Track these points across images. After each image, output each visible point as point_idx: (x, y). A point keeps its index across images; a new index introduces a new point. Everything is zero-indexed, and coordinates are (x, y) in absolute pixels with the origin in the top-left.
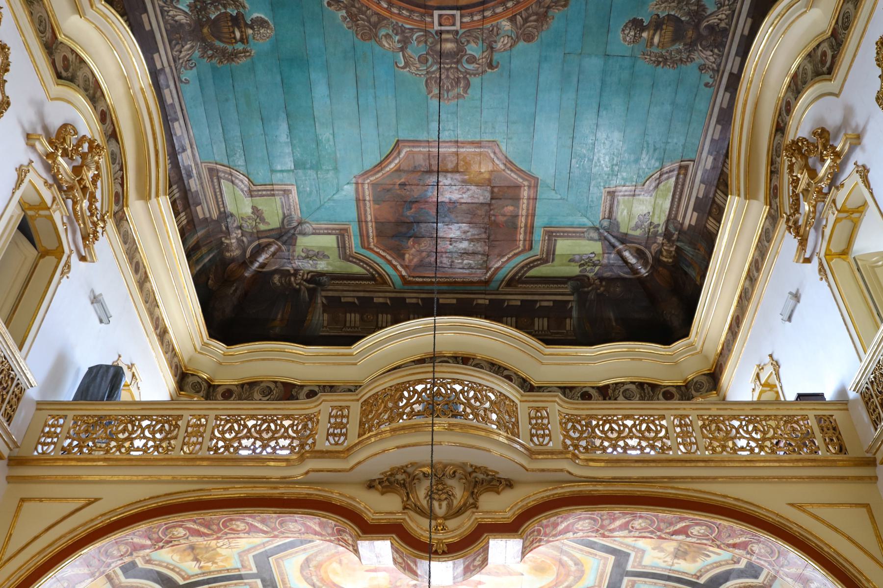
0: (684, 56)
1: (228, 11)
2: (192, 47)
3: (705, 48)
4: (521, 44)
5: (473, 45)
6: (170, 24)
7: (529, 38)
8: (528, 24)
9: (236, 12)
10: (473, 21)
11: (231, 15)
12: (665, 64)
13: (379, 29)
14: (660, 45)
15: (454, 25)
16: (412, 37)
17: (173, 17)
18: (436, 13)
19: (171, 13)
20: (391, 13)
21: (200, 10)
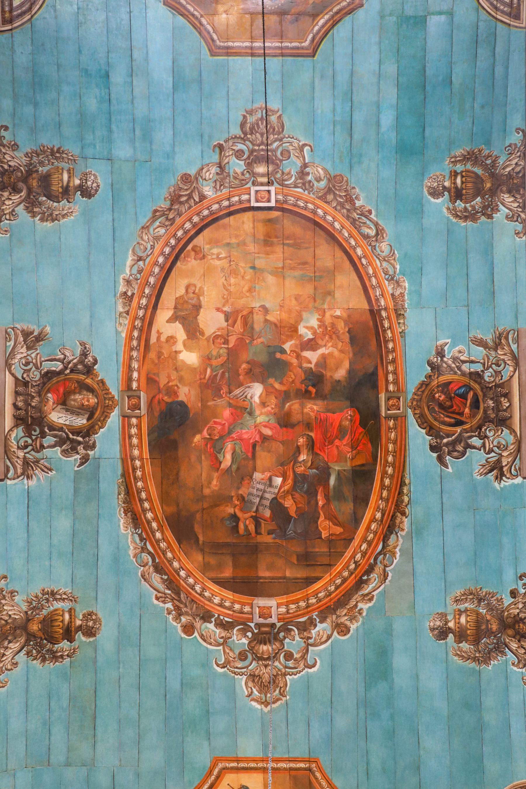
0: (35, 159)
1: (463, 205)
2: (504, 169)
3: (16, 169)
4: (193, 172)
5: (239, 170)
6: (520, 194)
7: (186, 178)
8: (188, 192)
9: (456, 204)
10: (239, 195)
11: (461, 201)
12: (52, 150)
13: (325, 188)
14: (61, 171)
15: (257, 192)
16: (296, 179)
17: (515, 201)
18: (273, 204)
19: (516, 205)
20: (313, 203)
21: (489, 206)
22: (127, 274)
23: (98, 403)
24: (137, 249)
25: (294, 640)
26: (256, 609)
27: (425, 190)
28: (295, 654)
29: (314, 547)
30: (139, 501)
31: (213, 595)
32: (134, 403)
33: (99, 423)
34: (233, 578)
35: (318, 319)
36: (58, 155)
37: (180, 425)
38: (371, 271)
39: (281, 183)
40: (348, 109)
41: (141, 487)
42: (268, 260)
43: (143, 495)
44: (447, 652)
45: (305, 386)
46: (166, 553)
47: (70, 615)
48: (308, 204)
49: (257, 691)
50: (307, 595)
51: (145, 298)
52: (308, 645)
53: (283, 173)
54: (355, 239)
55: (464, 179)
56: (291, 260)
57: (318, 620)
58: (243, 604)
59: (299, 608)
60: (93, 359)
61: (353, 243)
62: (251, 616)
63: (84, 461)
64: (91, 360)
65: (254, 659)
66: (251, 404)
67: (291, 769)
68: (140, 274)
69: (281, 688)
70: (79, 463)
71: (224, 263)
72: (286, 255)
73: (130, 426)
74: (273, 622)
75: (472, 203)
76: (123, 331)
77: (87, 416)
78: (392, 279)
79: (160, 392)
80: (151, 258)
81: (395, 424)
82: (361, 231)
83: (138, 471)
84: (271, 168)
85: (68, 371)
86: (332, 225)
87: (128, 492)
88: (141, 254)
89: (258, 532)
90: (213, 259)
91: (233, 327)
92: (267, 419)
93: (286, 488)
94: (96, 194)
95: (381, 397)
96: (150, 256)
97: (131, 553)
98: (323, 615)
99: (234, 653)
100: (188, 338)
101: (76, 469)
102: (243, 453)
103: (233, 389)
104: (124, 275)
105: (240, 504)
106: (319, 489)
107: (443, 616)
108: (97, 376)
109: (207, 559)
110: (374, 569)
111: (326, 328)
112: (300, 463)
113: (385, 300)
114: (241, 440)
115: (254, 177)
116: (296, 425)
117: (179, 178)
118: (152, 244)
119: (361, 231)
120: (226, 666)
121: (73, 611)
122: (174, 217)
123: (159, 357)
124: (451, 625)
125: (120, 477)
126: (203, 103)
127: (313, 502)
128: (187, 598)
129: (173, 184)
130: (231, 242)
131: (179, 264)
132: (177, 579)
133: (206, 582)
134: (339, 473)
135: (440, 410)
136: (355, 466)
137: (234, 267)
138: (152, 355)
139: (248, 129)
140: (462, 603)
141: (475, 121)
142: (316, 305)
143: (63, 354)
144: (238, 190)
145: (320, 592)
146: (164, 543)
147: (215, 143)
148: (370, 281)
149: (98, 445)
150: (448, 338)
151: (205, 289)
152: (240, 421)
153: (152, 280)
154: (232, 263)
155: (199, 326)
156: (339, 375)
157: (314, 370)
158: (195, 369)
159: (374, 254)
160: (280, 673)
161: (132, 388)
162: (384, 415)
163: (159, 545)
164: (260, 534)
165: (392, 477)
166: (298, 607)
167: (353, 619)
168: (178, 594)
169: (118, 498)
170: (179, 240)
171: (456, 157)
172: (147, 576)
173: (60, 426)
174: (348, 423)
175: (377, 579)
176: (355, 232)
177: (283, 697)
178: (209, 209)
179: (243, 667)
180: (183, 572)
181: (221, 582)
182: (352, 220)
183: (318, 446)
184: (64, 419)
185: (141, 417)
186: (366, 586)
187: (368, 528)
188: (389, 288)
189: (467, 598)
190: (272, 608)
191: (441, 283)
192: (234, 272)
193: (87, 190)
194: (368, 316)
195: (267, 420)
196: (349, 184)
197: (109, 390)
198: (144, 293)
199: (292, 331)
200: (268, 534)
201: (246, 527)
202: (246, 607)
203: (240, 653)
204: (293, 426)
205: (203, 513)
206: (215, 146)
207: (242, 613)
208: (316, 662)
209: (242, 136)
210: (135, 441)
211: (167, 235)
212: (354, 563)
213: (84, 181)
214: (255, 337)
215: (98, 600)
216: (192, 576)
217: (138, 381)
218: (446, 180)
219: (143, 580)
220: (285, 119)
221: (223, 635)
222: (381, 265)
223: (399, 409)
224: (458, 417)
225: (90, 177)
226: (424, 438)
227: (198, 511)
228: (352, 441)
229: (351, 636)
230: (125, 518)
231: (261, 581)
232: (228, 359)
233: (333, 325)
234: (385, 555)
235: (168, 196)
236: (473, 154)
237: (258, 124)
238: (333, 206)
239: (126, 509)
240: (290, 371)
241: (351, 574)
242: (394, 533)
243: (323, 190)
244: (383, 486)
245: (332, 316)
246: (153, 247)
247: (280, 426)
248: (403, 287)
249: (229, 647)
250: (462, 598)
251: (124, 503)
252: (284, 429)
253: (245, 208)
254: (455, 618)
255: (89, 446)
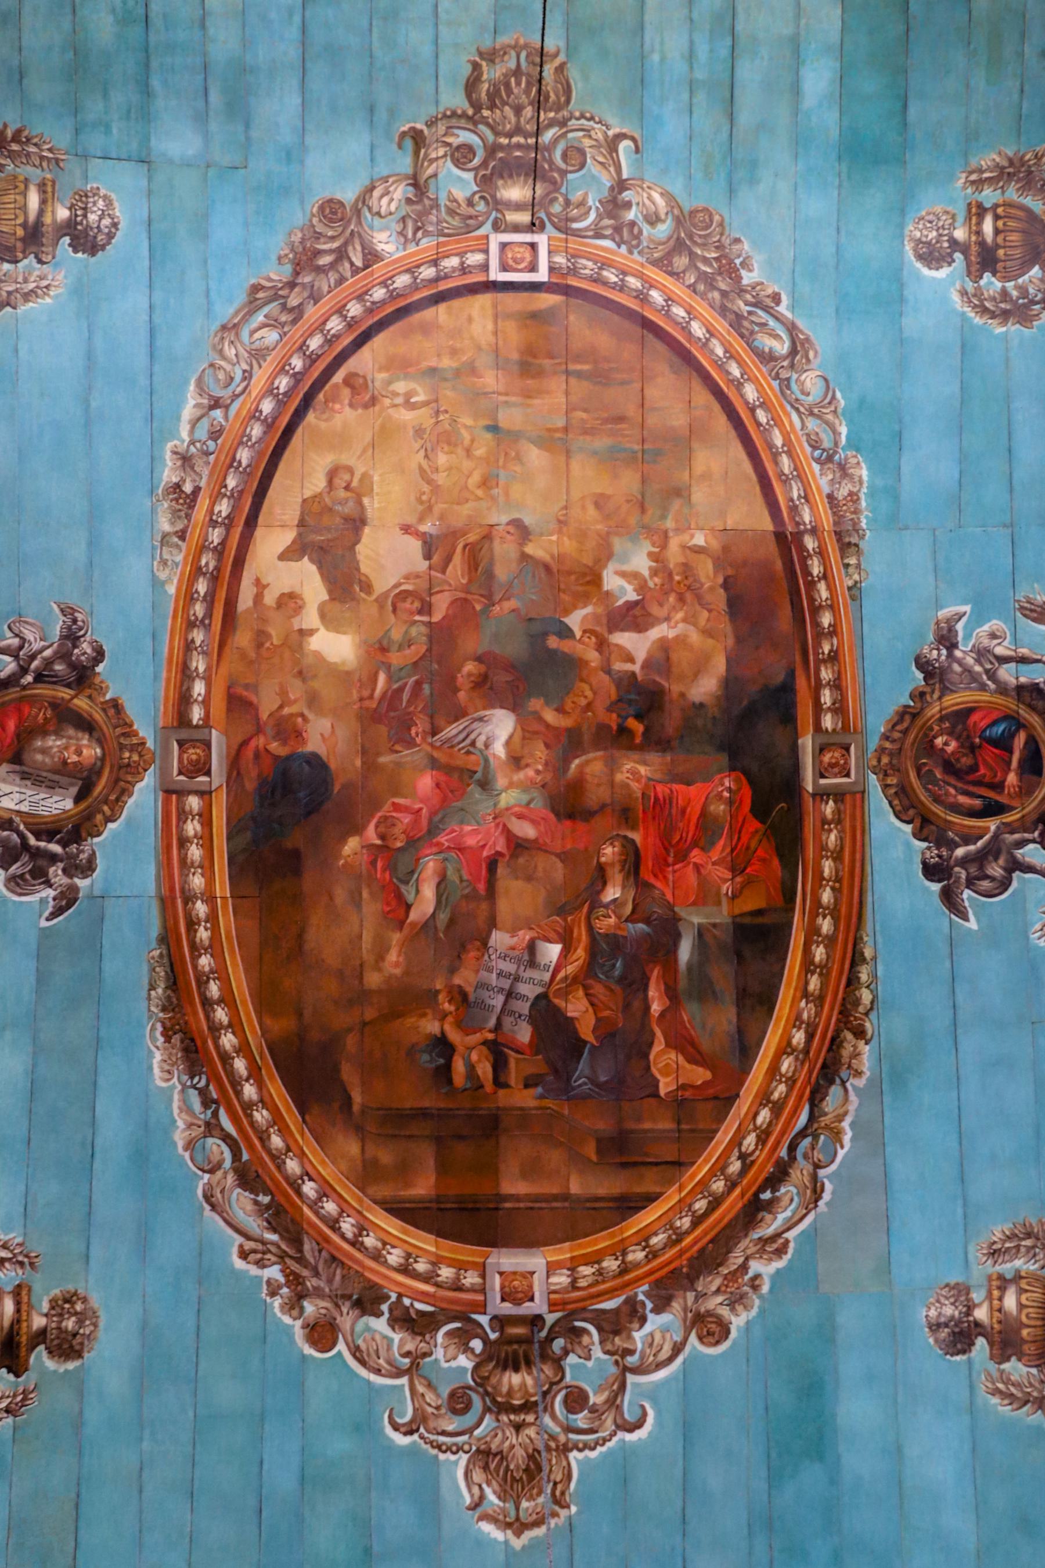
4: (348, 195)
7: (331, 210)
10: (461, 254)
13: (669, 239)
15: (504, 246)
20: (640, 276)
22: (183, 441)
23: (103, 759)
24: (209, 380)
25: (588, 1358)
26: (493, 1278)
27: (907, 248)
28: (591, 1395)
29: (639, 1119)
30: (203, 1005)
31: (385, 1244)
32: (194, 757)
33: (106, 808)
34: (438, 1199)
35: (650, 555)
36: (15, 147)
37: (309, 813)
38: (778, 441)
39: (564, 226)
40: (724, 52)
41: (207, 969)
42: (529, 410)
43: (214, 989)
44: (972, 1387)
45: (619, 716)
46: (269, 1136)
47: (18, 1304)
48: (628, 278)
49: (495, 1492)
50: (623, 1240)
51: (225, 500)
52: (626, 1369)
53: (567, 203)
54: (741, 363)
55: (1000, 223)
56: (585, 410)
57: (649, 1305)
58: (461, 1266)
59: (601, 1274)
60: (93, 649)
61: (735, 371)
62: (481, 1298)
63: (64, 903)
64: (89, 651)
65: (487, 1410)
66: (486, 760)
68: (215, 440)
69: (555, 1484)
70: (50, 910)
71: (423, 417)
72: (574, 399)
73: (183, 815)
74: (537, 1312)
75: (1020, 281)
76: (169, 580)
77: (74, 790)
78: (830, 459)
79: (259, 730)
80: (243, 403)
81: (838, 812)
82: (756, 343)
83: (202, 929)
84: (539, 192)
85: (29, 678)
86: (685, 329)
87: (175, 981)
88: (218, 393)
89: (499, 1083)
90: (395, 406)
91: (444, 572)
92: (525, 798)
93: (570, 969)
94: (109, 243)
95: (803, 744)
96: (242, 398)
97: (179, 1138)
98: (663, 1292)
99: (438, 1396)
100: (332, 599)
101: (44, 924)
102: (465, 884)
103: (442, 723)
104: (176, 442)
105: (457, 1009)
106: (652, 971)
107: (960, 1292)
108: (102, 690)
109: (371, 1150)
110: (786, 1174)
111: (670, 575)
112: (606, 906)
113: (811, 509)
114: (460, 850)
115: (498, 210)
116: (596, 812)
117: (315, 210)
118: (246, 367)
119: (756, 343)
120: (417, 1430)
121: (24, 1293)
122: (301, 304)
123: (259, 645)
124: (981, 1314)
125: (154, 944)
126: (375, 30)
127: (637, 1004)
128: (320, 1251)
129: (301, 223)
130: (441, 366)
131: (311, 417)
132: (293, 1204)
133: (369, 1210)
134: (701, 933)
135: (947, 778)
136: (742, 915)
137: (447, 426)
138: (242, 639)
139: (483, 95)
140: (1007, 1257)
141: (1026, 88)
142: (647, 519)
143: (17, 635)
144: (458, 242)
145: (656, 1234)
146: (265, 1112)
147: (405, 128)
148: (776, 463)
149: (100, 861)
150: (965, 602)
151: (376, 478)
152: (458, 804)
153: (244, 456)
154: (441, 417)
155: (358, 569)
156: (702, 690)
157: (640, 678)
158: (348, 673)
159: (785, 398)
160: (553, 1445)
161: (191, 721)
162: (810, 789)
163: (251, 1116)
164: (506, 1086)
165: (830, 942)
166: (600, 1272)
167: (736, 1301)
168: (297, 1242)
169: (149, 998)
170: (312, 359)
171: (981, 171)
172: (219, 1196)
173: (6, 815)
174: (722, 807)
175: (796, 1199)
176: (739, 346)
177: (562, 1507)
178: (387, 287)
179: (460, 1429)
180: (311, 1184)
181: (408, 1209)
182: (733, 317)
183: (650, 864)
184: (17, 797)
185: (211, 792)
186: (768, 1217)
187: (774, 1069)
188: (822, 481)
189: (1018, 1247)
190: (536, 1276)
191: (946, 472)
192: (448, 439)
193: (87, 235)
194: (771, 548)
195: (524, 802)
196: (727, 232)
197: (131, 725)
198: (226, 486)
199: (588, 583)
200: (527, 1086)
201: (471, 1068)
202: (469, 1273)
203: (452, 1395)
204: (588, 815)
205: (362, 1034)
206: (403, 134)
207: (460, 1288)
208: (645, 1414)
209: (470, 112)
210: (195, 852)
211: (283, 347)
212: (739, 1158)
213: (79, 213)
214: (497, 597)
215: (92, 1262)
216: (334, 1195)
217: (206, 703)
218: (957, 224)
219: (207, 1207)
220: (574, 74)
221: (410, 1346)
222: (803, 427)
223: (848, 775)
224: (991, 794)
225: (95, 203)
226: (908, 845)
227: (350, 1030)
228: (732, 851)
229: (731, 1347)
230: (165, 1049)
231: (508, 1205)
232: (429, 650)
233: (687, 569)
234: (816, 1137)
235: (287, 251)
236: (1023, 165)
237: (507, 85)
238: (687, 283)
239: (168, 1024)
240: (582, 680)
241: (732, 1185)
242: (838, 1081)
243: (664, 243)
244: (808, 966)
245: (684, 547)
246: (247, 376)
247: (557, 815)
248: (857, 479)
249: (425, 1378)
250: (1007, 1245)
251: (164, 1009)
252: (568, 823)
253: (475, 284)
254: (989, 1296)
255: (77, 867)
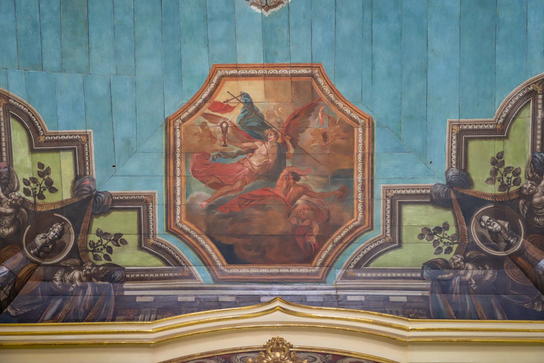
67: (293, 75)
